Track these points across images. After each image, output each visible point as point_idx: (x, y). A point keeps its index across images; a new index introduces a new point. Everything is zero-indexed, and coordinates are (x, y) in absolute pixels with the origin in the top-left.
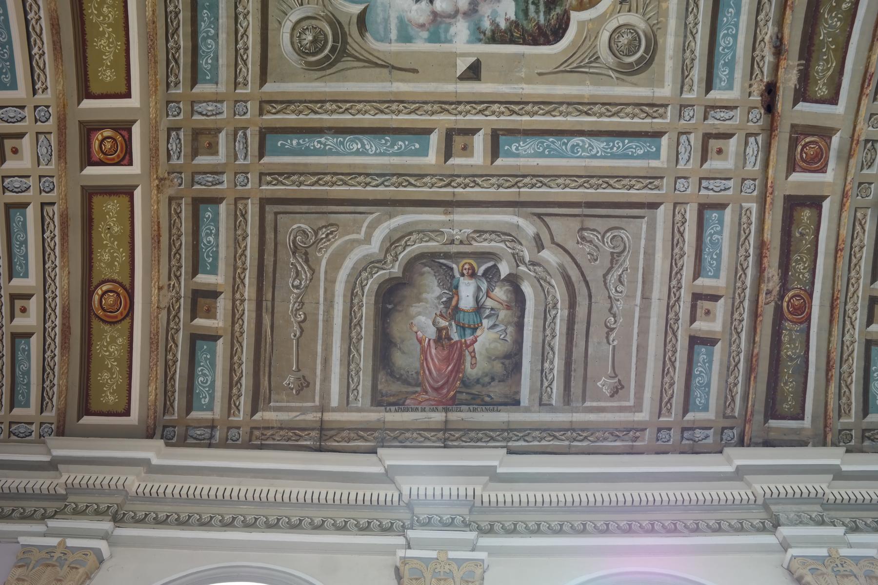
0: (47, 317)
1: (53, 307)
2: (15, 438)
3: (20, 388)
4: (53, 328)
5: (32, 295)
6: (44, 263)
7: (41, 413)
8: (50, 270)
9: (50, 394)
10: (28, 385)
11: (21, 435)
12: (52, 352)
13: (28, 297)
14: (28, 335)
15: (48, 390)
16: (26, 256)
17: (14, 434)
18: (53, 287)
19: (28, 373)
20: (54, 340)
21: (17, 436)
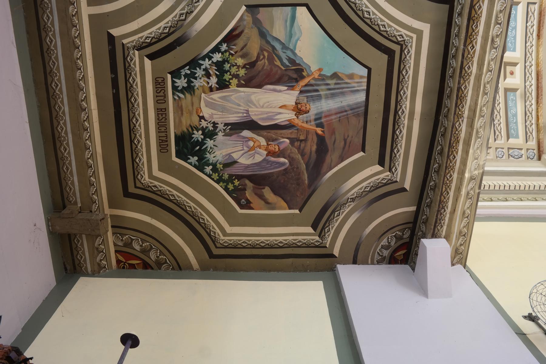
0: (527, 79)
1: (530, 72)
2: (513, 159)
3: (512, 125)
4: (531, 86)
5: (517, 64)
6: (526, 43)
7: (526, 142)
8: (529, 47)
9: (531, 130)
10: (516, 123)
11: (516, 157)
12: (530, 102)
13: (515, 64)
14: (515, 90)
15: (529, 127)
16: (515, 37)
17: (511, 156)
18: (530, 59)
19: (515, 115)
20: (531, 94)
21: (513, 157)
